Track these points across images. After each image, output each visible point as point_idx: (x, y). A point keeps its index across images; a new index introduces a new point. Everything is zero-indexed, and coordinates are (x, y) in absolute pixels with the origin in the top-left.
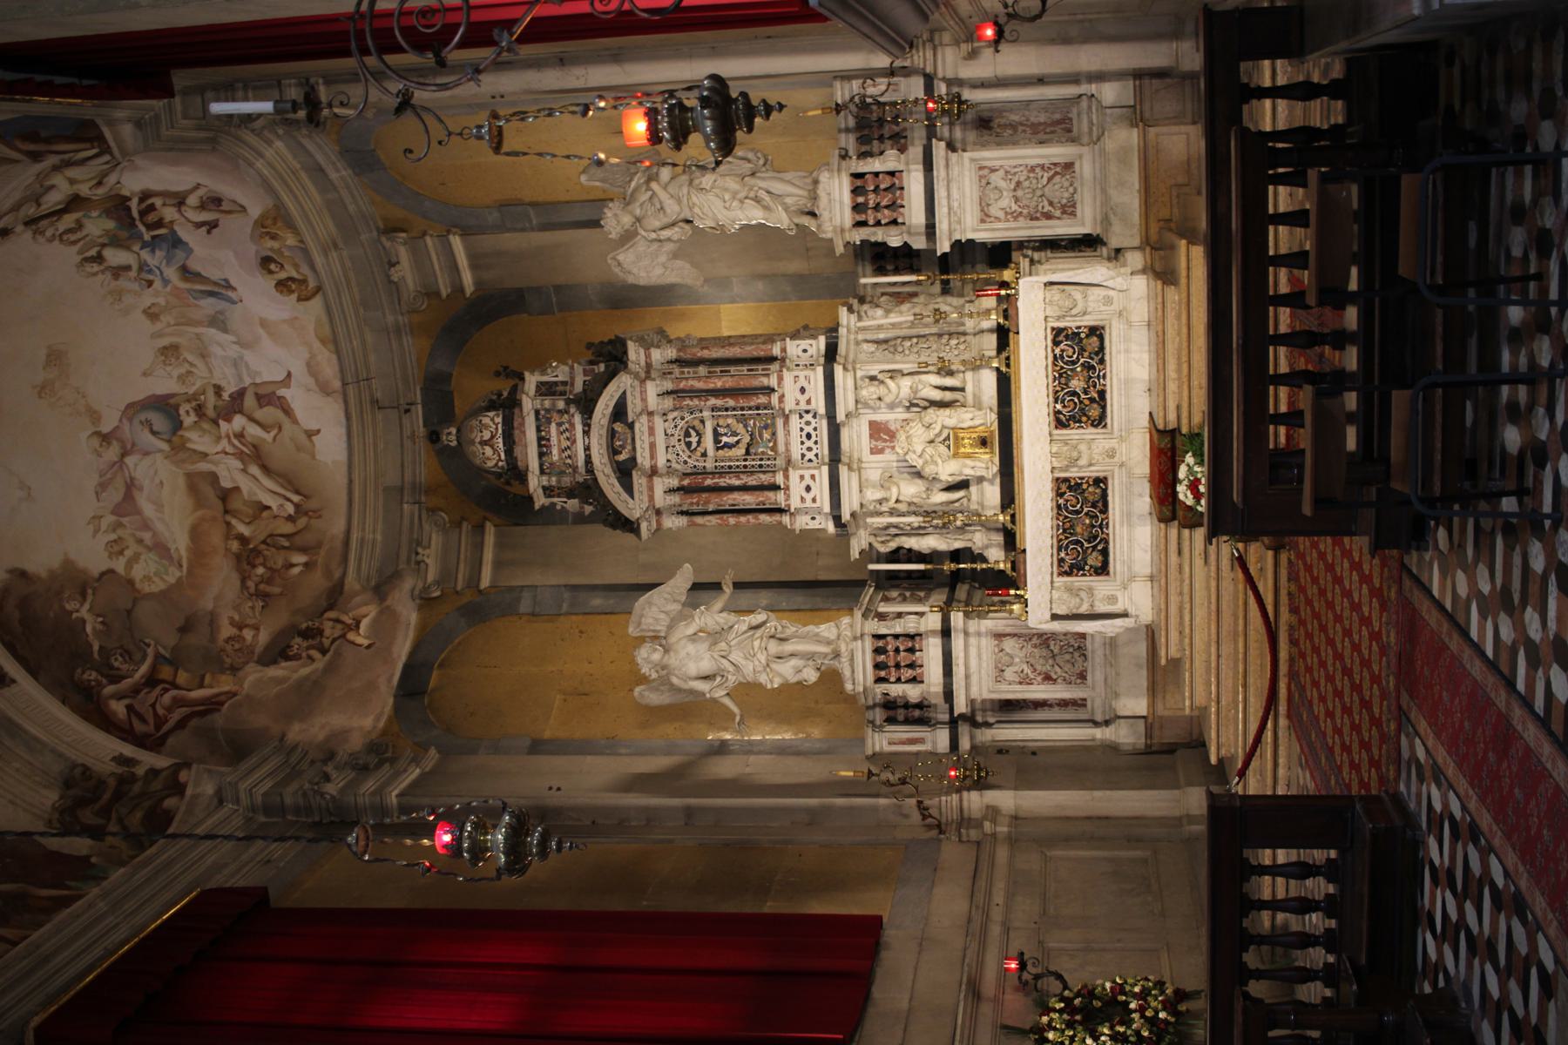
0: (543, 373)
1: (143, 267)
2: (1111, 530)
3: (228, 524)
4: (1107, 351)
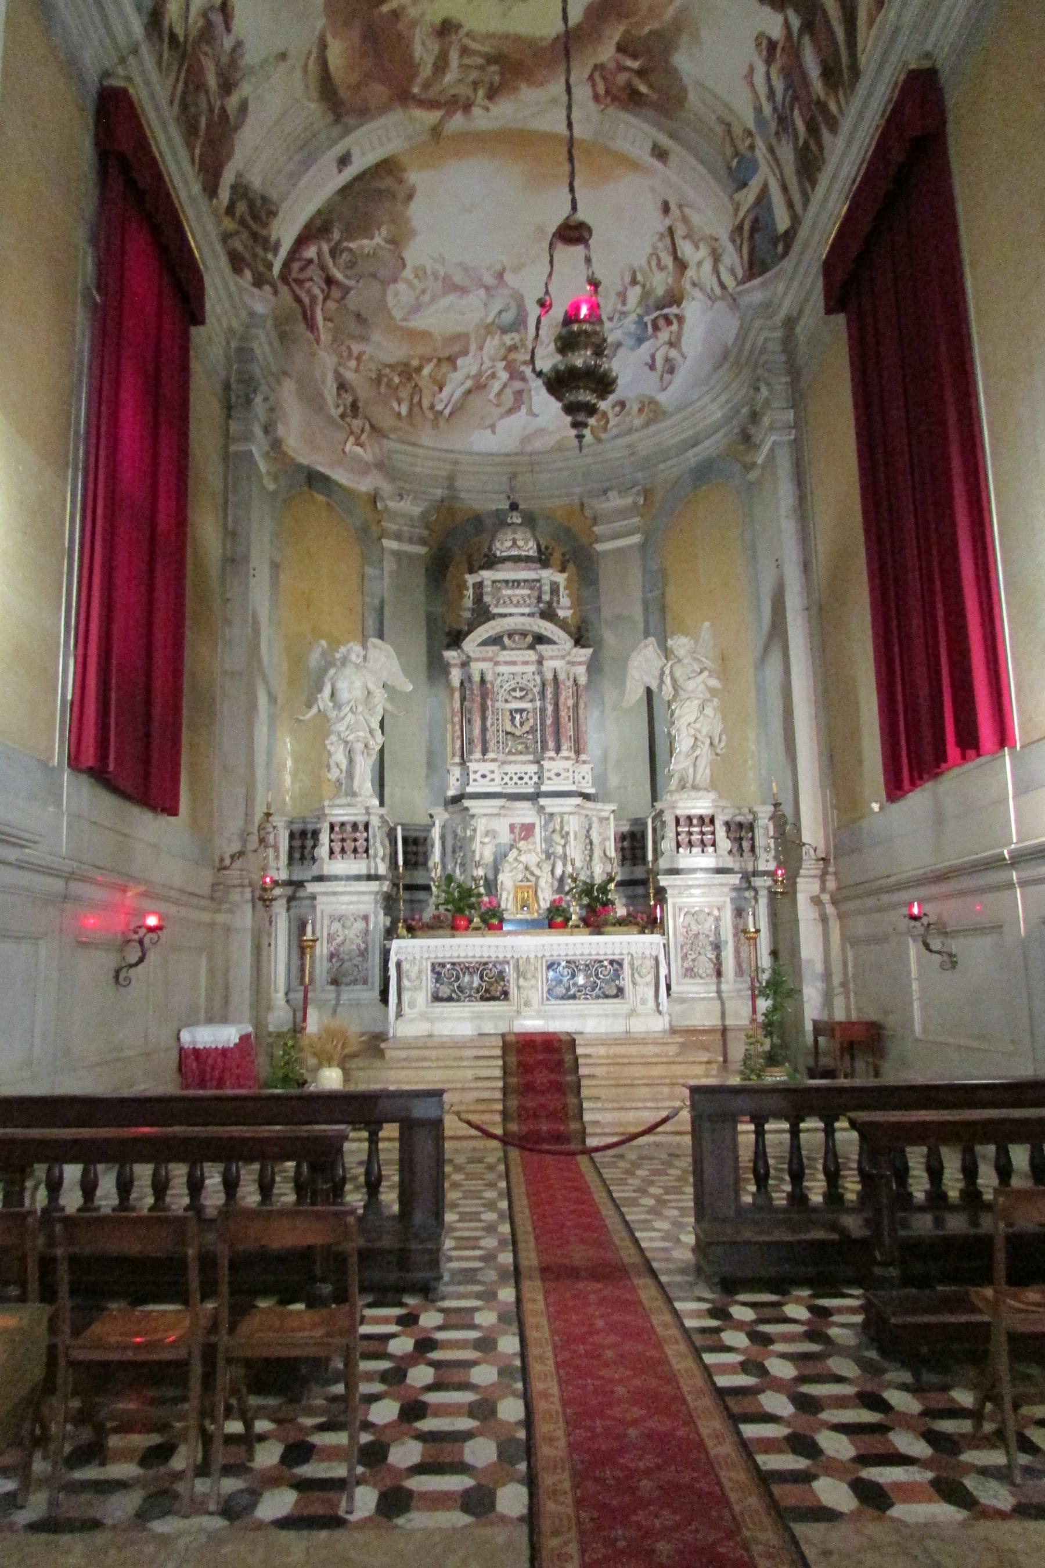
0: (566, 588)
1: (624, 314)
2: (467, 1003)
3: (430, 360)
4: (606, 1001)
